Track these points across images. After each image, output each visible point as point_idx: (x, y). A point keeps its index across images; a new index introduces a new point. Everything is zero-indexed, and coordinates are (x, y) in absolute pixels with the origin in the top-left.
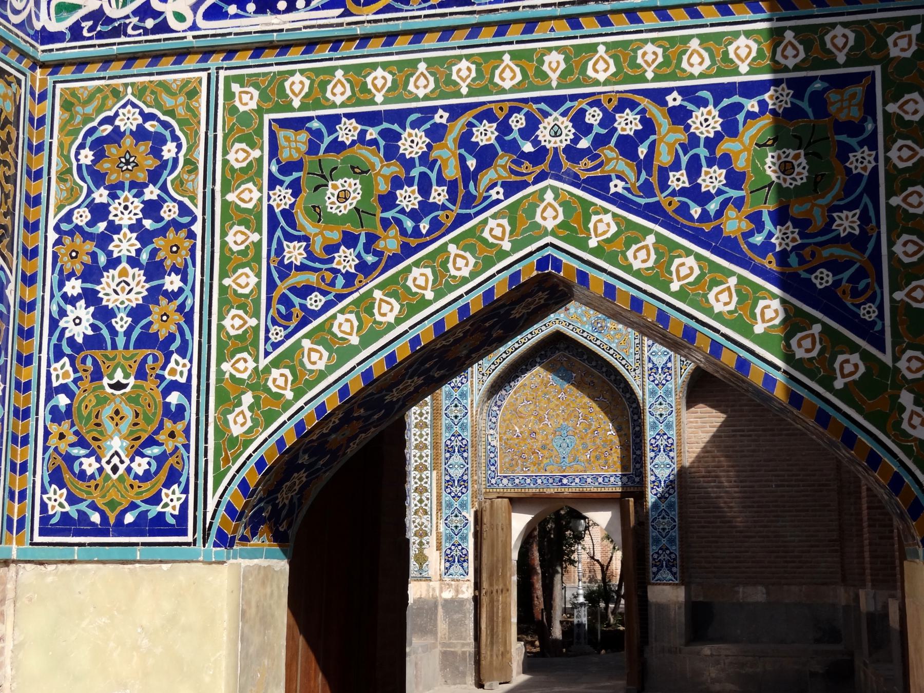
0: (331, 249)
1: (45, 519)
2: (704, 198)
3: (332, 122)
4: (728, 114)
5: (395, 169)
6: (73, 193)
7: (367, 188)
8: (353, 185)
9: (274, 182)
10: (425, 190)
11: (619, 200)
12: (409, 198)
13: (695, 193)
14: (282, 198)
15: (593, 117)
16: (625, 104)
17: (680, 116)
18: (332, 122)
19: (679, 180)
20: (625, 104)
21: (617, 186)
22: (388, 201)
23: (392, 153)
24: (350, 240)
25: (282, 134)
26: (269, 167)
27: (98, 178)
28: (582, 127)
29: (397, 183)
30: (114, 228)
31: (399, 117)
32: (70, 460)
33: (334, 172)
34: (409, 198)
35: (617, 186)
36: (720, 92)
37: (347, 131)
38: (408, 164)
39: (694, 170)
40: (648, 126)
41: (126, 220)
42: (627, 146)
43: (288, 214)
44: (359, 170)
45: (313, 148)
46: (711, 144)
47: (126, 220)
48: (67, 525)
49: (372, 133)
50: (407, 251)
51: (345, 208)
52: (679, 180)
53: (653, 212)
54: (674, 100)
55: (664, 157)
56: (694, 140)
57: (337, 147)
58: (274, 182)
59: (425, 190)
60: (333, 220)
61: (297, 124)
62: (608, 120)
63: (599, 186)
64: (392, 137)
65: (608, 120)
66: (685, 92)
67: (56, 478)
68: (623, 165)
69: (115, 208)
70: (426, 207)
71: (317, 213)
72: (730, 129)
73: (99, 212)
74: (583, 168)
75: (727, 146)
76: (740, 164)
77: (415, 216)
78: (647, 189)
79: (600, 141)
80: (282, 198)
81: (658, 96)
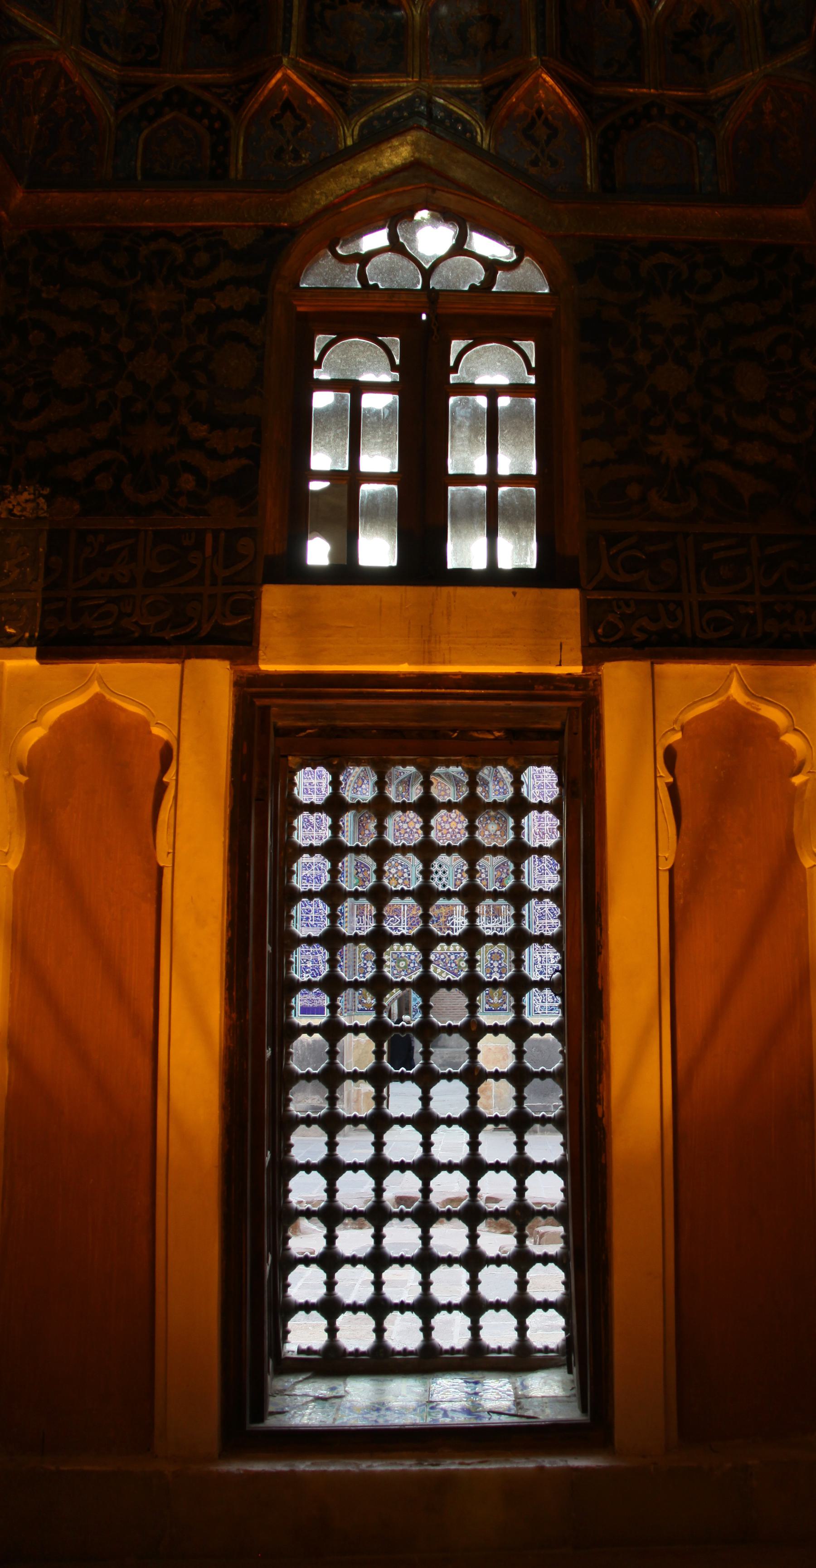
0: (401, 972)
1: (358, 1009)
2: (452, 968)
3: (401, 953)
4: (456, 956)
5: (410, 961)
6: (361, 961)
7: (406, 963)
8: (404, 963)
9: (392, 961)
10: (414, 964)
11: (441, 967)
12: (412, 965)
13: (451, 967)
14: (393, 964)
15: (438, 955)
16: (442, 954)
17: (449, 956)
18: (401, 953)
19: (449, 965)
20: (442, 954)
21: (441, 965)
22: (409, 965)
23: (409, 958)
24: (403, 971)
25: (393, 954)
26: (391, 959)
27: (365, 959)
28: (436, 957)
29: (410, 963)
30: (367, 967)
31: (411, 953)
32: (362, 1001)
33: (401, 961)
34: (412, 965)
35: (441, 965)
36: (455, 953)
37: (403, 955)
38: (412, 960)
39: (451, 964)
40: (445, 957)
41: (369, 966)
42: (442, 960)
43: (394, 966)
44: (405, 960)
45: (398, 957)
46: (453, 960)
47: (369, 966)
48: (362, 1010)
49: (407, 955)
50: (412, 973)
51: (403, 966)
52: (449, 965)
53: (445, 969)
54: (449, 954)
55: (447, 962)
56: (451, 960)
57: (401, 957)
58: (392, 961)
59: (414, 964)
60: (401, 968)
61: (396, 953)
62: (440, 956)
63: (438, 965)
64: (409, 956)
65: (440, 956)
66: (450, 953)
67: (360, 1003)
68: (442, 962)
69: (368, 964)
70: (414, 967)
71: (399, 966)
72: (456, 958)
73: (365, 964)
74: (436, 963)
75: (456, 961)
76: (457, 963)
77: (413, 968)
78: (445, 966)
79: (439, 959)
80: (393, 964)
81: (446, 953)
